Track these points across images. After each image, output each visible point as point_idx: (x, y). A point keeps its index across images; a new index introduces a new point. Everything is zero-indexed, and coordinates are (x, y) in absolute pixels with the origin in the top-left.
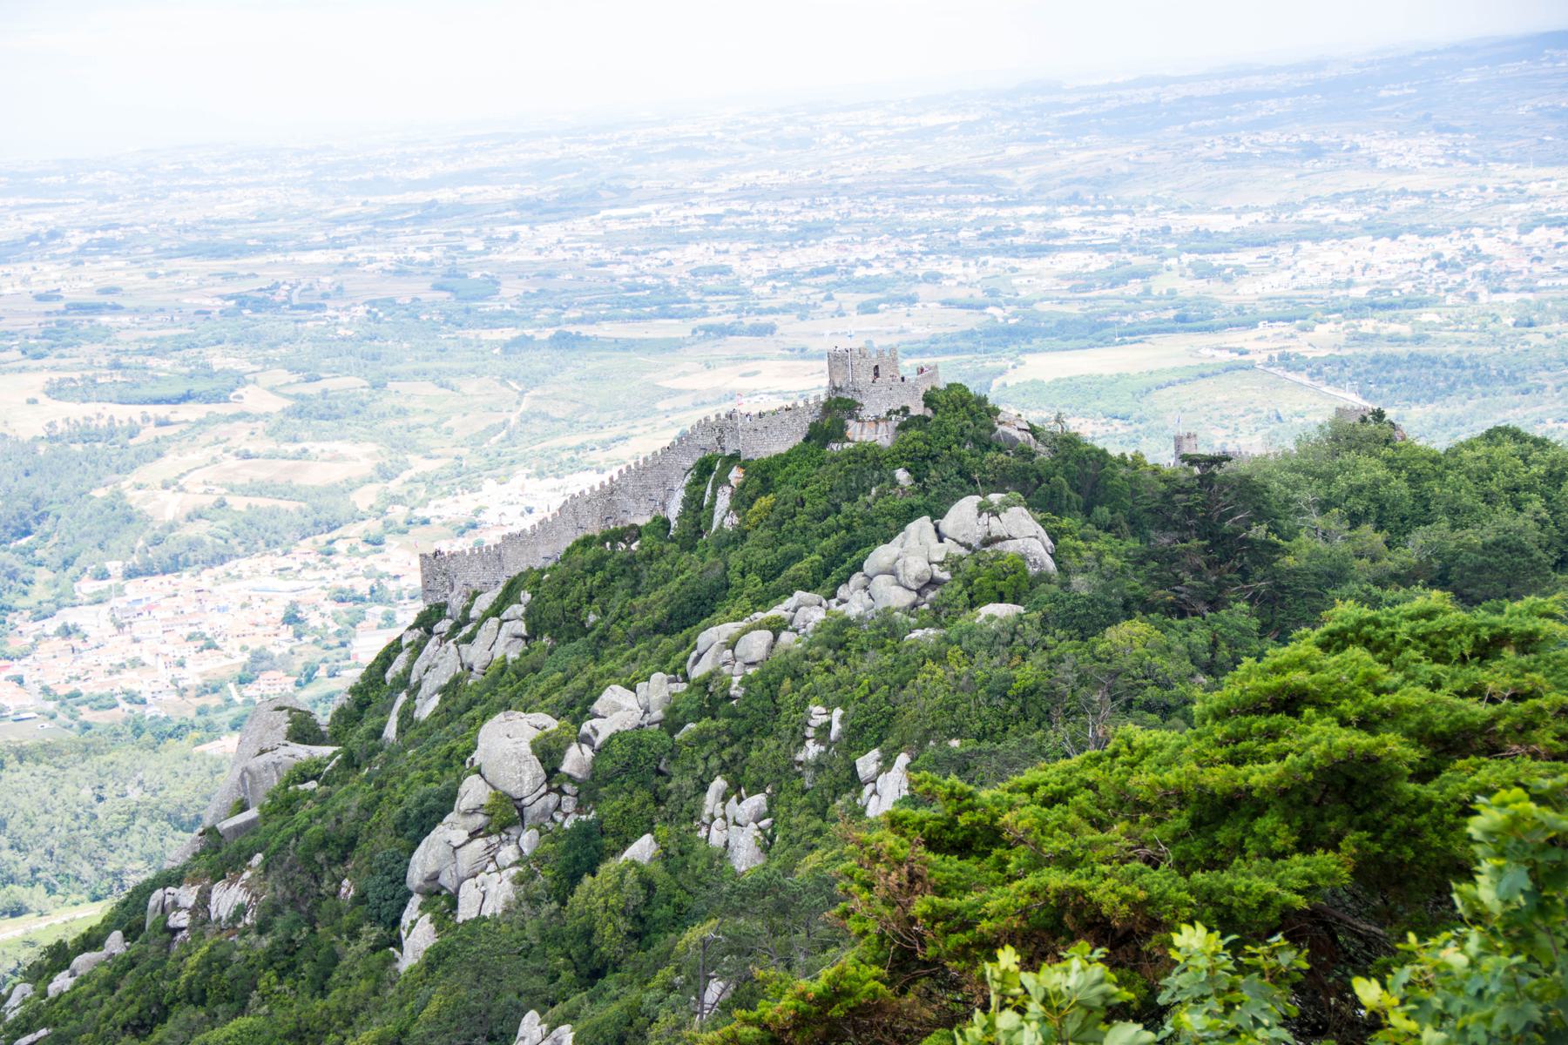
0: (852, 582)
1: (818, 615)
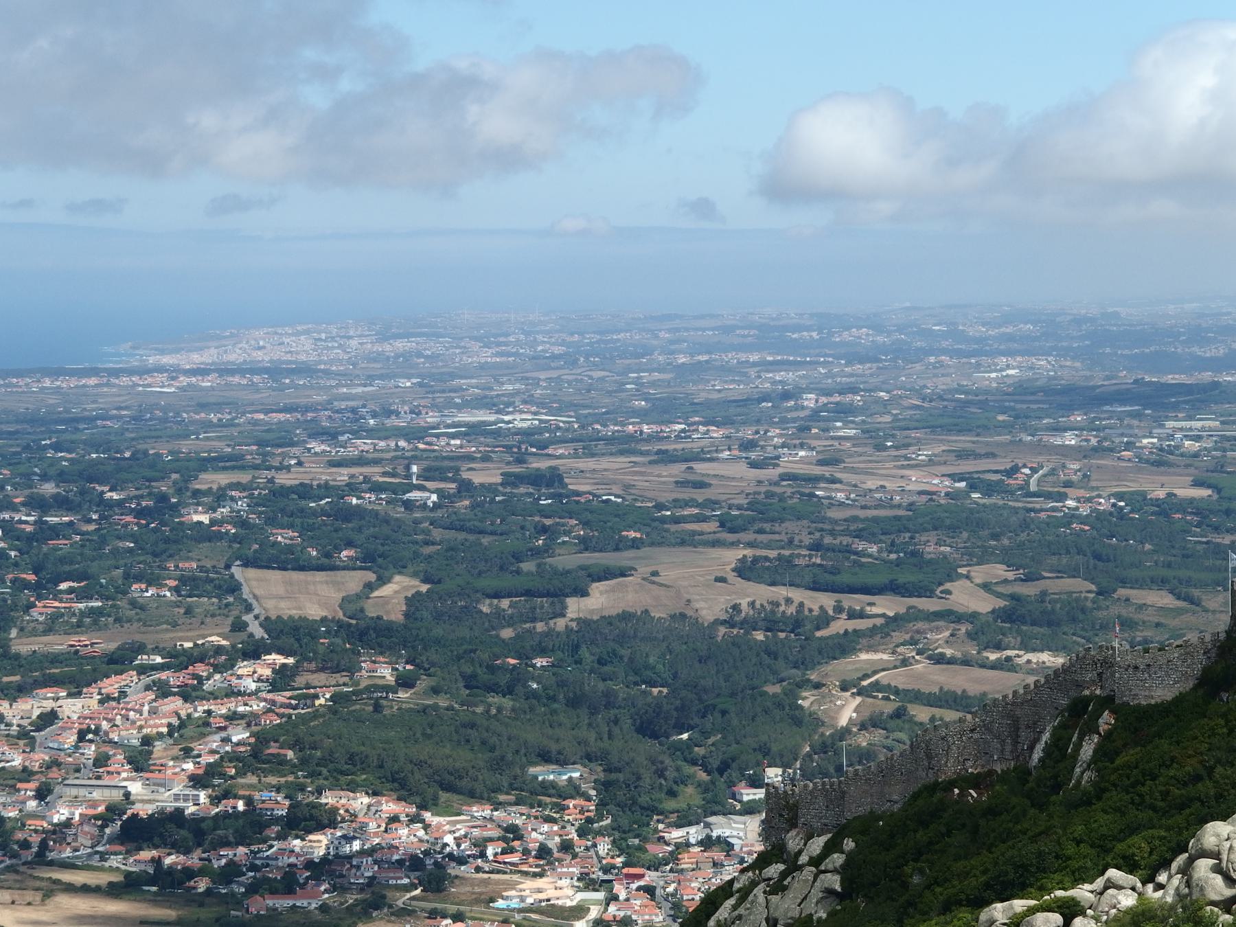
0: (1175, 866)
1: (1127, 900)
